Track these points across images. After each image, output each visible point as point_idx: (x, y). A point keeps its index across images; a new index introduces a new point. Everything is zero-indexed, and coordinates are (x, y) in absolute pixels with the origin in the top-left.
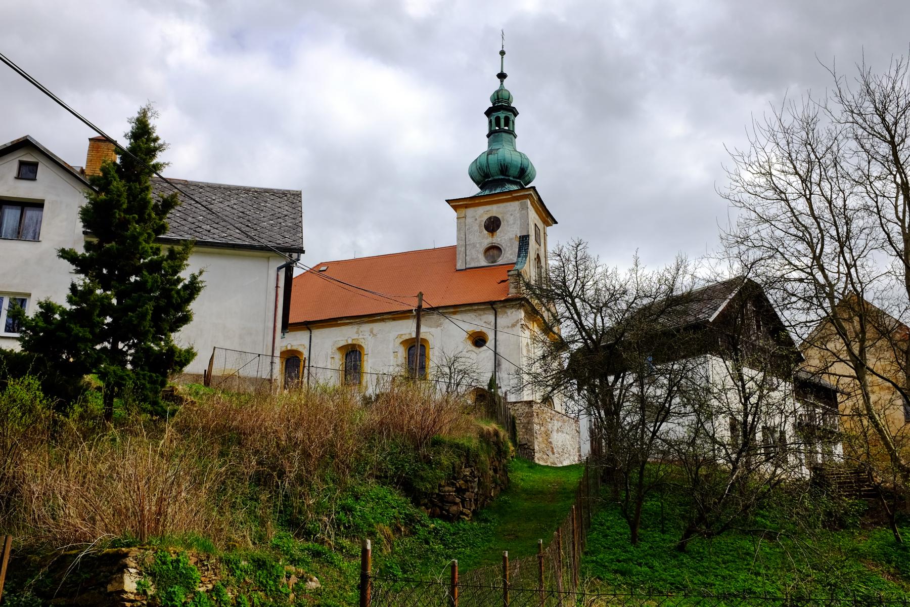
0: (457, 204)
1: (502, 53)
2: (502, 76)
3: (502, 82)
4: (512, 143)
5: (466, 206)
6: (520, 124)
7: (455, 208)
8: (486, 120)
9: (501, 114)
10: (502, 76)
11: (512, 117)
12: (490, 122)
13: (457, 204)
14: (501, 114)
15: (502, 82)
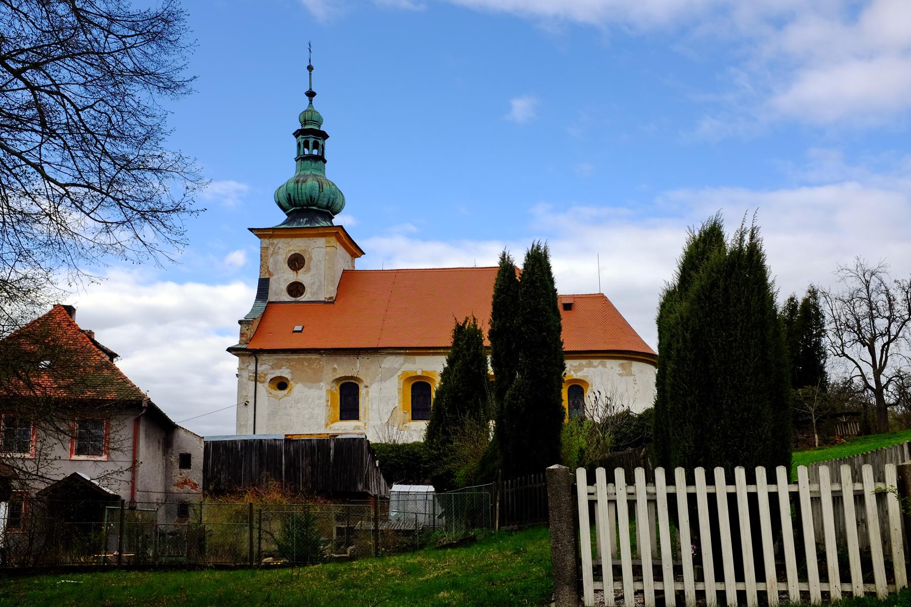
0: (261, 233)
1: (310, 68)
2: (311, 94)
3: (311, 101)
4: (322, 170)
5: (271, 237)
6: (330, 148)
7: (259, 236)
8: (294, 141)
9: (311, 137)
10: (311, 94)
11: (321, 142)
12: (299, 145)
13: (261, 233)
14: (311, 137)
15: (311, 101)
